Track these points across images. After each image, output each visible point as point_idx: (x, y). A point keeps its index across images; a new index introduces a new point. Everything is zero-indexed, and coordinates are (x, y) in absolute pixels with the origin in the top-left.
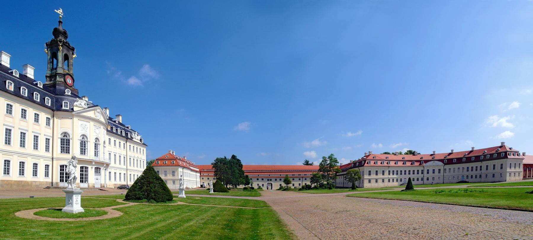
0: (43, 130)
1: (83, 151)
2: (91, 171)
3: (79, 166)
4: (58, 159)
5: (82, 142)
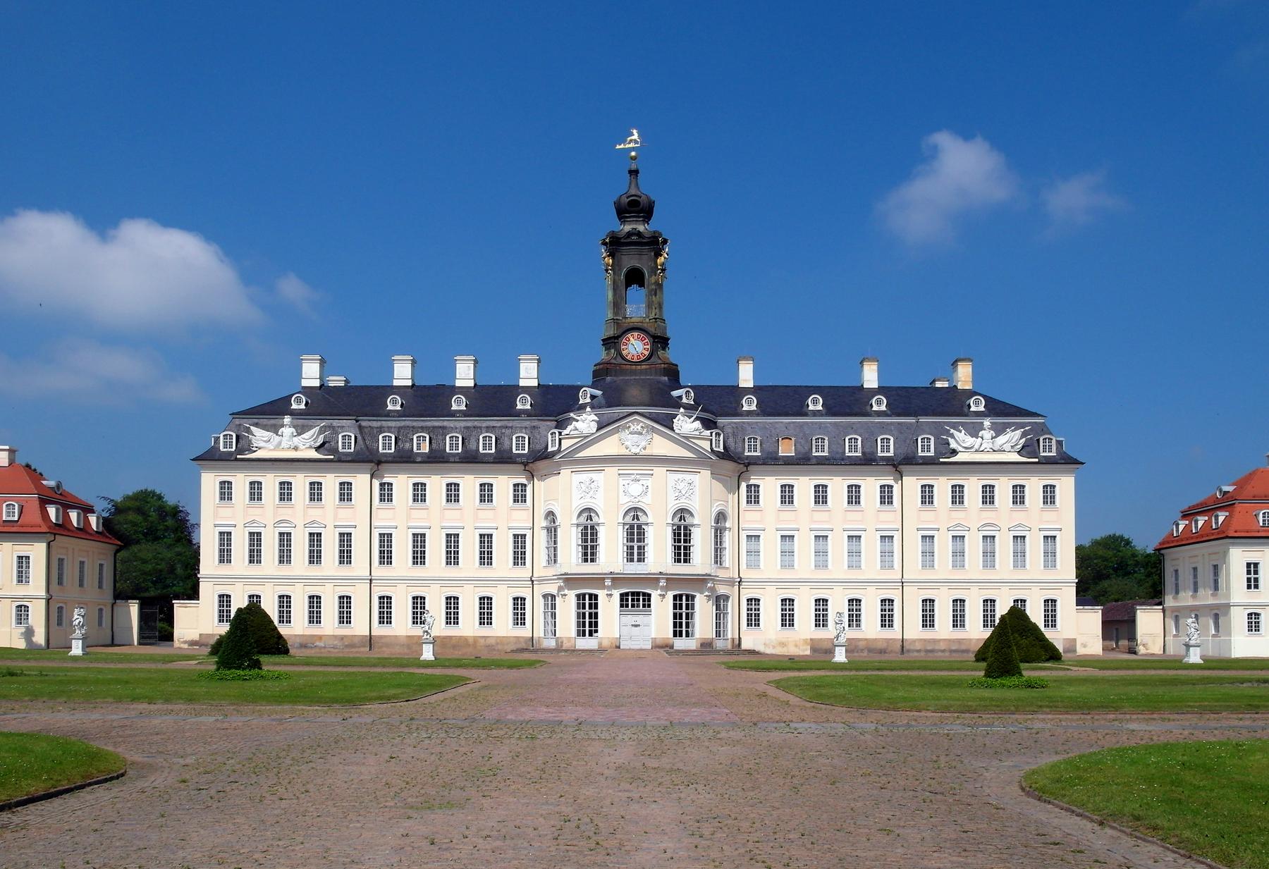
0: (505, 517)
1: (589, 553)
2: (608, 605)
3: (571, 595)
4: (542, 580)
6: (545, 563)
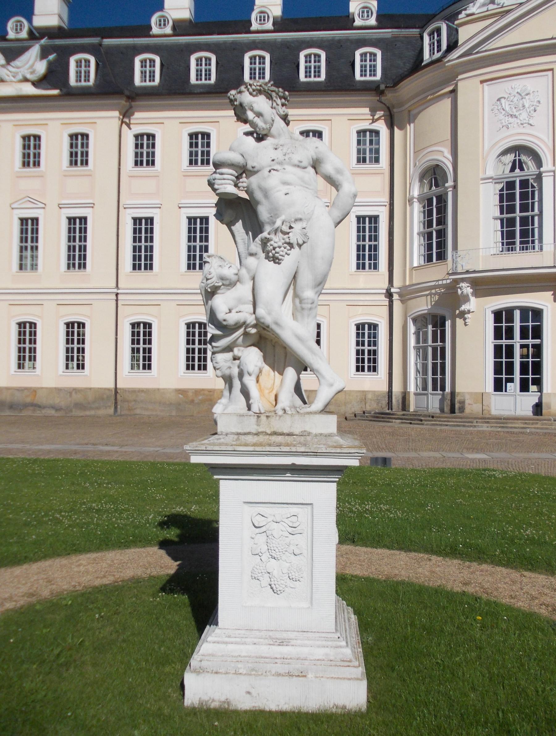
5: (510, 185)
6: (417, 259)
